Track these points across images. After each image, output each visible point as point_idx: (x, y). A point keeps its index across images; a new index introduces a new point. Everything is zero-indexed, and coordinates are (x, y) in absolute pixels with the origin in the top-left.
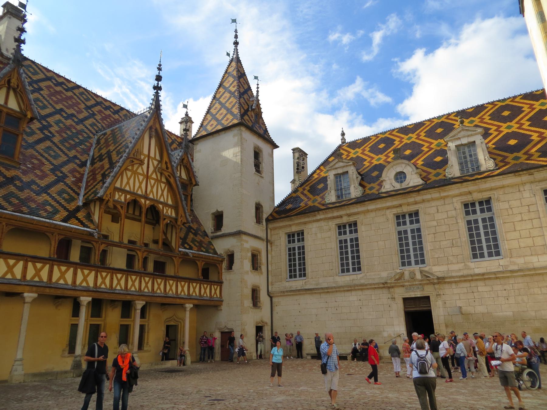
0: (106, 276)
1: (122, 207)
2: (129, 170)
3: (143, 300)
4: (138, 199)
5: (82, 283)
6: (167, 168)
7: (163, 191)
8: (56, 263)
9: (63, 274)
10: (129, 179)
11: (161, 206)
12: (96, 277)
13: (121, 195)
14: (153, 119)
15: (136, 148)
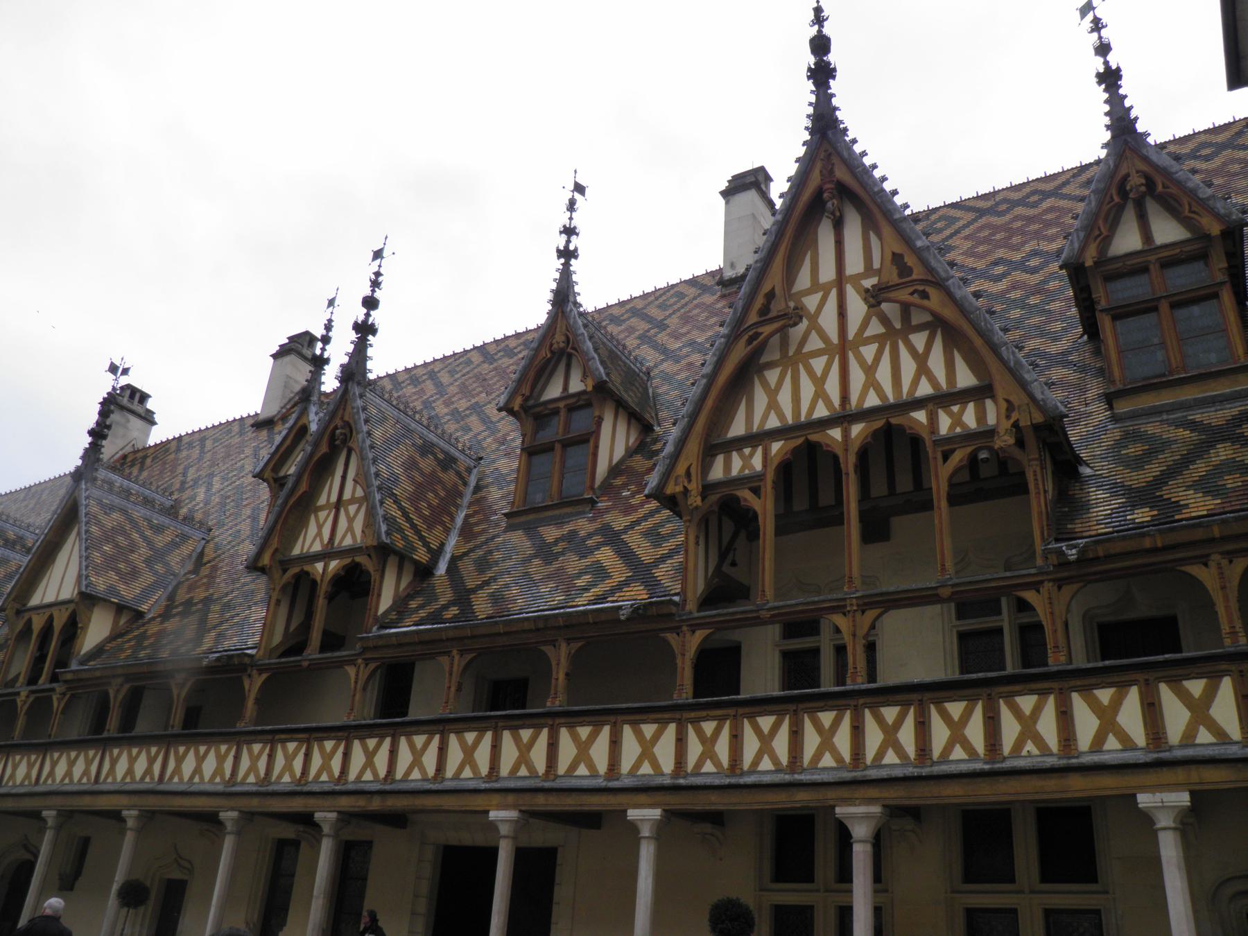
0: (717, 732)
1: (756, 491)
2: (770, 365)
3: (870, 801)
4: (814, 437)
5: (637, 765)
6: (904, 270)
7: (921, 361)
8: (562, 720)
9: (583, 749)
10: (773, 394)
11: (921, 416)
12: (681, 741)
13: (751, 455)
14: (819, 165)
15: (766, 288)
